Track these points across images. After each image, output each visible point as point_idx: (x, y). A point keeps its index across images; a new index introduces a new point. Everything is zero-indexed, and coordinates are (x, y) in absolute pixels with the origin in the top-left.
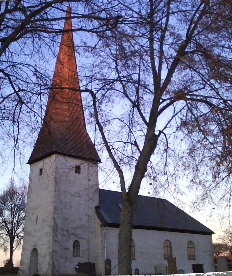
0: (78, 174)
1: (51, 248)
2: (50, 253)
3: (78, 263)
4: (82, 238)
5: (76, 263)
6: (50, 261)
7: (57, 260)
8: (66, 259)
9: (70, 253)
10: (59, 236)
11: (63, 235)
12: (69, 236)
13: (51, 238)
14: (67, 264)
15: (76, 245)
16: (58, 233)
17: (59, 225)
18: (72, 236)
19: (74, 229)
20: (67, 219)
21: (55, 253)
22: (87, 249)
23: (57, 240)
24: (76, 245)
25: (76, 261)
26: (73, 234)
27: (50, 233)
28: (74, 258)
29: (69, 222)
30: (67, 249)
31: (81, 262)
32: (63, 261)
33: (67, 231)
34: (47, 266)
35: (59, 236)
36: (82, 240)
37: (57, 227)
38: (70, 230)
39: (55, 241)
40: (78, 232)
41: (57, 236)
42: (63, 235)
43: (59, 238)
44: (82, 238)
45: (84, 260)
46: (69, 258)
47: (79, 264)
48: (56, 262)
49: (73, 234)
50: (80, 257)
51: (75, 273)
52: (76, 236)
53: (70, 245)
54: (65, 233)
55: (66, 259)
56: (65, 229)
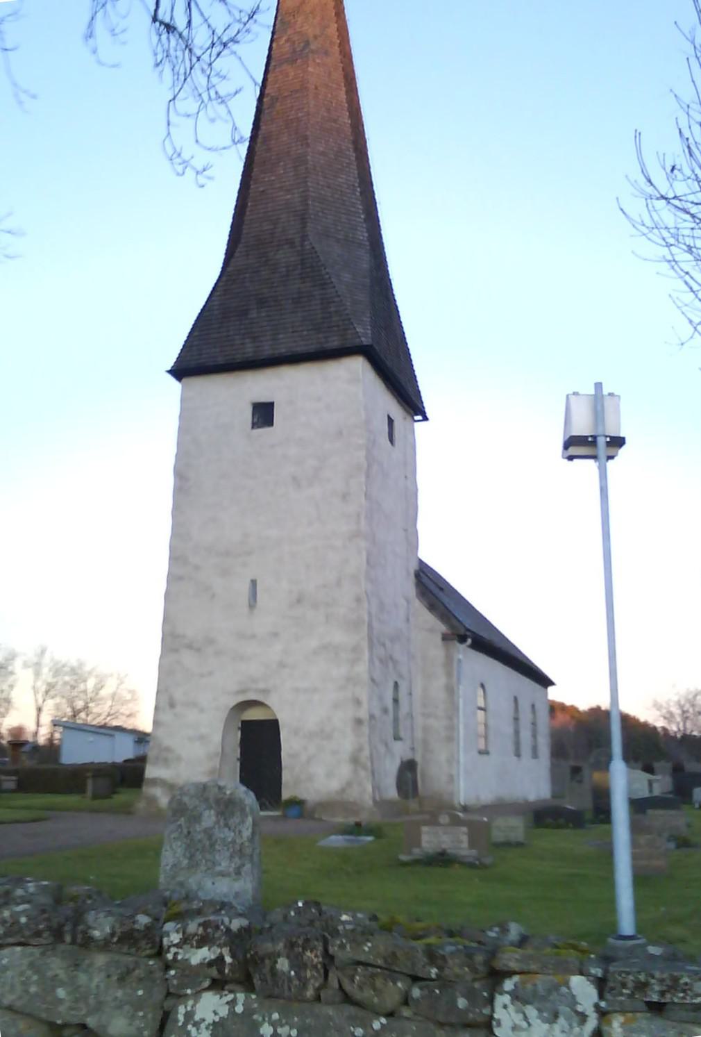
1: (365, 705)
2: (359, 722)
6: (360, 749)
13: (362, 669)
27: (356, 649)
34: (345, 771)
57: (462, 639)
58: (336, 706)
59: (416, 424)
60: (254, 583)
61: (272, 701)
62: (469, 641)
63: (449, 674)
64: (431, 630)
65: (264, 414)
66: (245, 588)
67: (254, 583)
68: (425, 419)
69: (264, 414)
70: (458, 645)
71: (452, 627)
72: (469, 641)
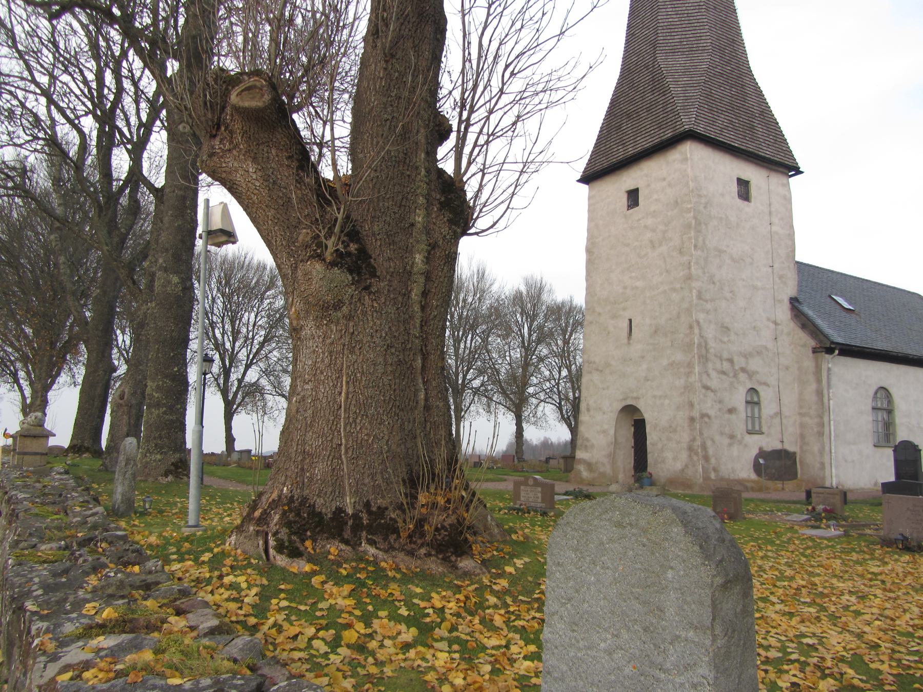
0: (746, 203)
3: (760, 449)
4: (766, 384)
5: (755, 452)
7: (713, 440)
8: (732, 437)
9: (739, 422)
10: (714, 374)
11: (724, 373)
12: (735, 376)
14: (735, 450)
15: (753, 400)
16: (710, 365)
17: (712, 344)
18: (742, 377)
19: (746, 356)
20: (726, 329)
21: (706, 419)
22: (776, 414)
23: (709, 384)
24: (753, 400)
25: (755, 444)
26: (743, 370)
28: (748, 436)
29: (733, 337)
30: (731, 411)
31: (765, 449)
32: (726, 441)
33: (731, 361)
35: (714, 374)
36: (764, 387)
37: (707, 350)
38: (736, 359)
39: (707, 388)
40: (755, 364)
41: (708, 375)
42: (724, 373)
43: (715, 381)
44: (766, 384)
45: (771, 443)
46: (739, 436)
47: (762, 453)
48: (709, 443)
49: (743, 370)
50: (763, 433)
51: (753, 476)
52: (751, 375)
53: (739, 398)
54: (726, 366)
55: (732, 437)
56: (725, 355)
57: (830, 351)
58: (678, 408)
59: (791, 180)
60: (630, 321)
61: (641, 405)
62: (837, 352)
63: (819, 381)
64: (804, 346)
65: (633, 196)
66: (626, 324)
67: (630, 321)
68: (798, 172)
69: (633, 196)
70: (827, 356)
71: (820, 341)
72: (837, 352)
